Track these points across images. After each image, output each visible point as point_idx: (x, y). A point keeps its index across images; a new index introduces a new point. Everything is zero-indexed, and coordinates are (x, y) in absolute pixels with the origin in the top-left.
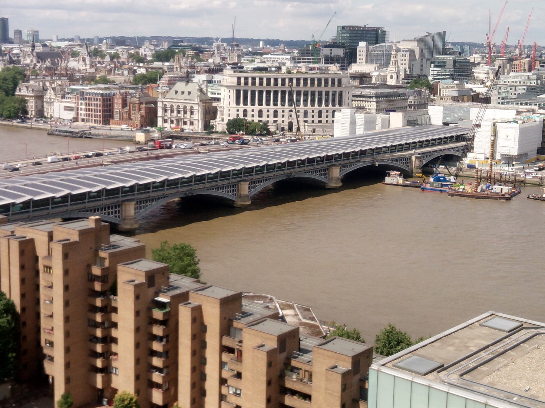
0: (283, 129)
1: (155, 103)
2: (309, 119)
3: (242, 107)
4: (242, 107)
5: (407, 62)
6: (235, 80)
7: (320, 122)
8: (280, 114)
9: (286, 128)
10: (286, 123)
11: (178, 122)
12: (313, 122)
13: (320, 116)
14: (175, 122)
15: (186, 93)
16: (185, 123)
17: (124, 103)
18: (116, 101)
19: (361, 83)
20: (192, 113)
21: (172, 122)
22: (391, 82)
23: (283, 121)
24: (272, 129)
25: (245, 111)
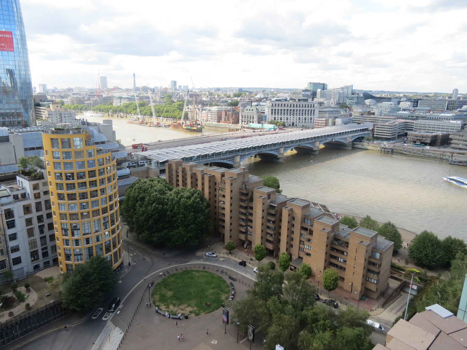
0: (290, 125)
1: (239, 114)
2: (301, 121)
3: (273, 116)
4: (273, 116)
5: (337, 97)
6: (271, 104)
7: (305, 122)
8: (289, 119)
9: (291, 124)
10: (292, 122)
11: (248, 122)
12: (302, 122)
13: (305, 120)
14: (246, 122)
15: (251, 110)
16: (250, 122)
17: (226, 115)
18: (223, 113)
19: (320, 106)
20: (253, 118)
21: (245, 122)
22: (333, 106)
23: (290, 122)
24: (286, 125)
25: (275, 118)
